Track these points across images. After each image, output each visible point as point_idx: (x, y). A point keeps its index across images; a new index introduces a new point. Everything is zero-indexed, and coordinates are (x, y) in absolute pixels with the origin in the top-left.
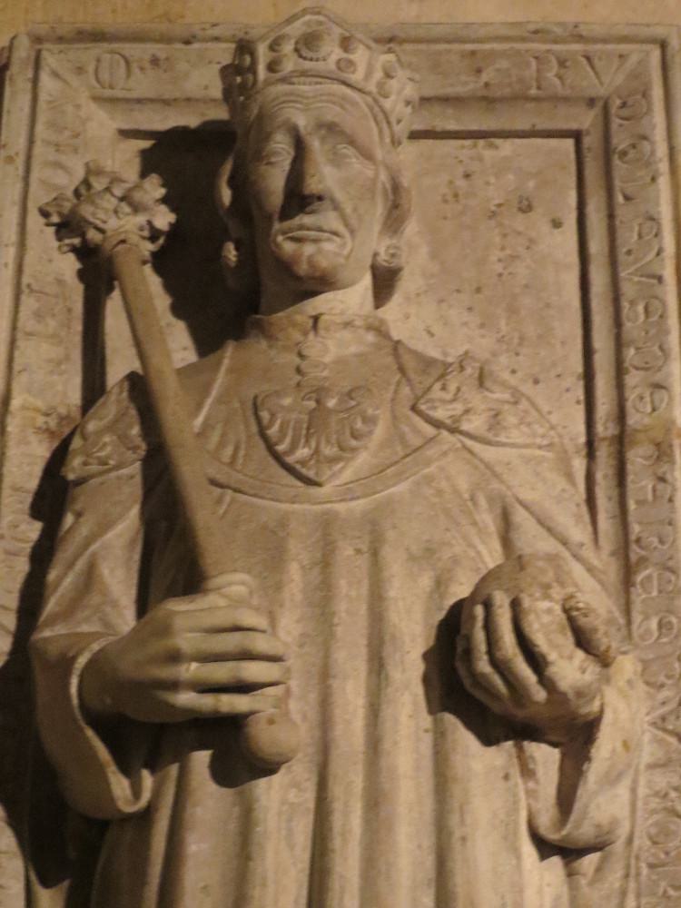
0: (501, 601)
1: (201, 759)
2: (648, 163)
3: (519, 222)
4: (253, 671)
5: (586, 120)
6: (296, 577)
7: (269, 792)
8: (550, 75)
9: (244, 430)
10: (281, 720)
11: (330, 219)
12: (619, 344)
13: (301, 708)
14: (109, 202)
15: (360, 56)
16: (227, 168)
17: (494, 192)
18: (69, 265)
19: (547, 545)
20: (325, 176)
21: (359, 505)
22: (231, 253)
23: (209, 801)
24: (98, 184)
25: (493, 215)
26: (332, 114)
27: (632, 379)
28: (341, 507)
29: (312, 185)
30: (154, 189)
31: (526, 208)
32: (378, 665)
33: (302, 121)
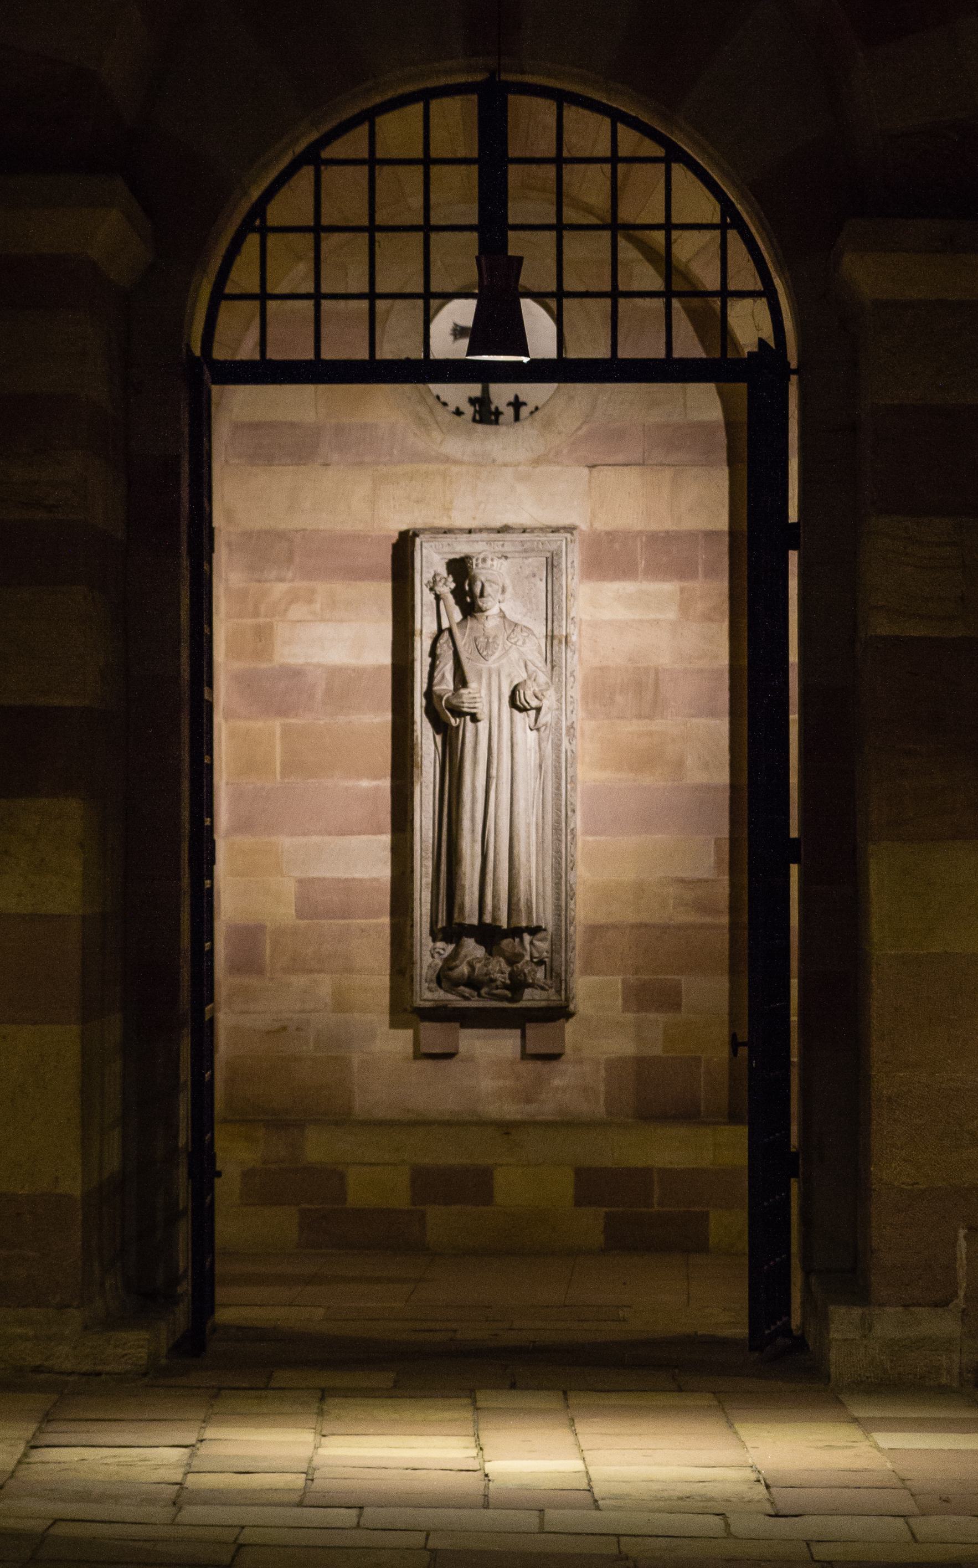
0: (522, 692)
1: (468, 718)
2: (560, 570)
3: (533, 580)
4: (476, 705)
5: (549, 555)
6: (484, 681)
7: (480, 725)
8: (540, 546)
9: (473, 645)
10: (482, 712)
11: (490, 598)
12: (553, 615)
13: (486, 710)
14: (441, 584)
15: (495, 563)
16: (467, 582)
17: (527, 571)
18: (432, 596)
19: (534, 668)
20: (488, 589)
21: (496, 665)
22: (468, 600)
23: (470, 725)
24: (438, 579)
25: (526, 578)
26: (490, 577)
27: (555, 623)
28: (492, 666)
29: (485, 594)
30: (451, 579)
31: (534, 576)
32: (500, 700)
33: (483, 579)
